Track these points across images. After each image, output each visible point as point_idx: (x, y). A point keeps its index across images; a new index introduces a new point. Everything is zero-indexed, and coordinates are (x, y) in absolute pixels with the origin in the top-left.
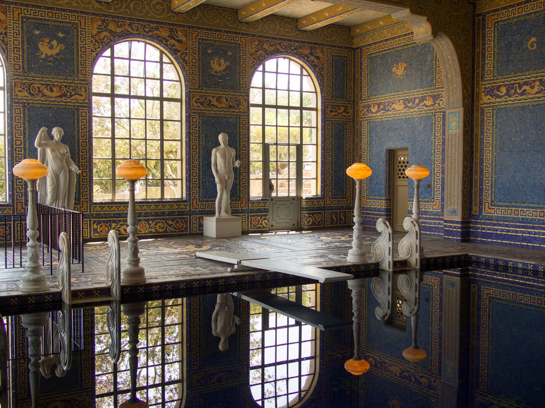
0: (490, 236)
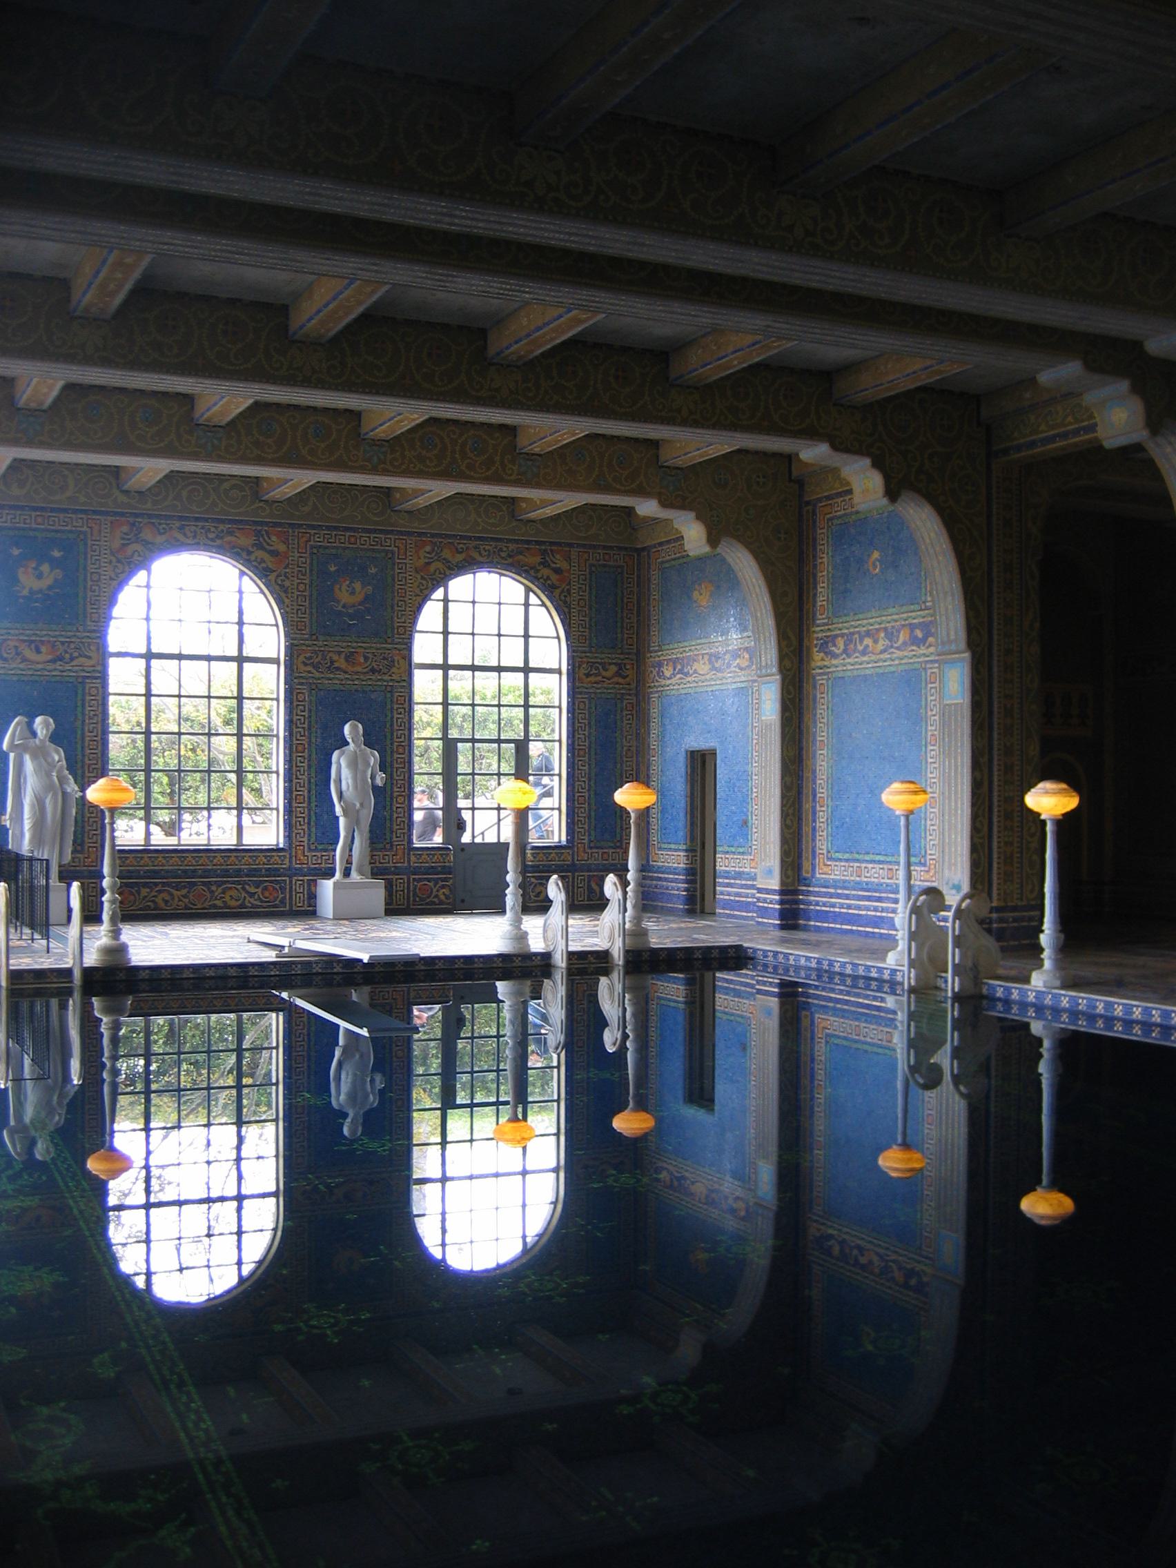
0: (837, 917)
